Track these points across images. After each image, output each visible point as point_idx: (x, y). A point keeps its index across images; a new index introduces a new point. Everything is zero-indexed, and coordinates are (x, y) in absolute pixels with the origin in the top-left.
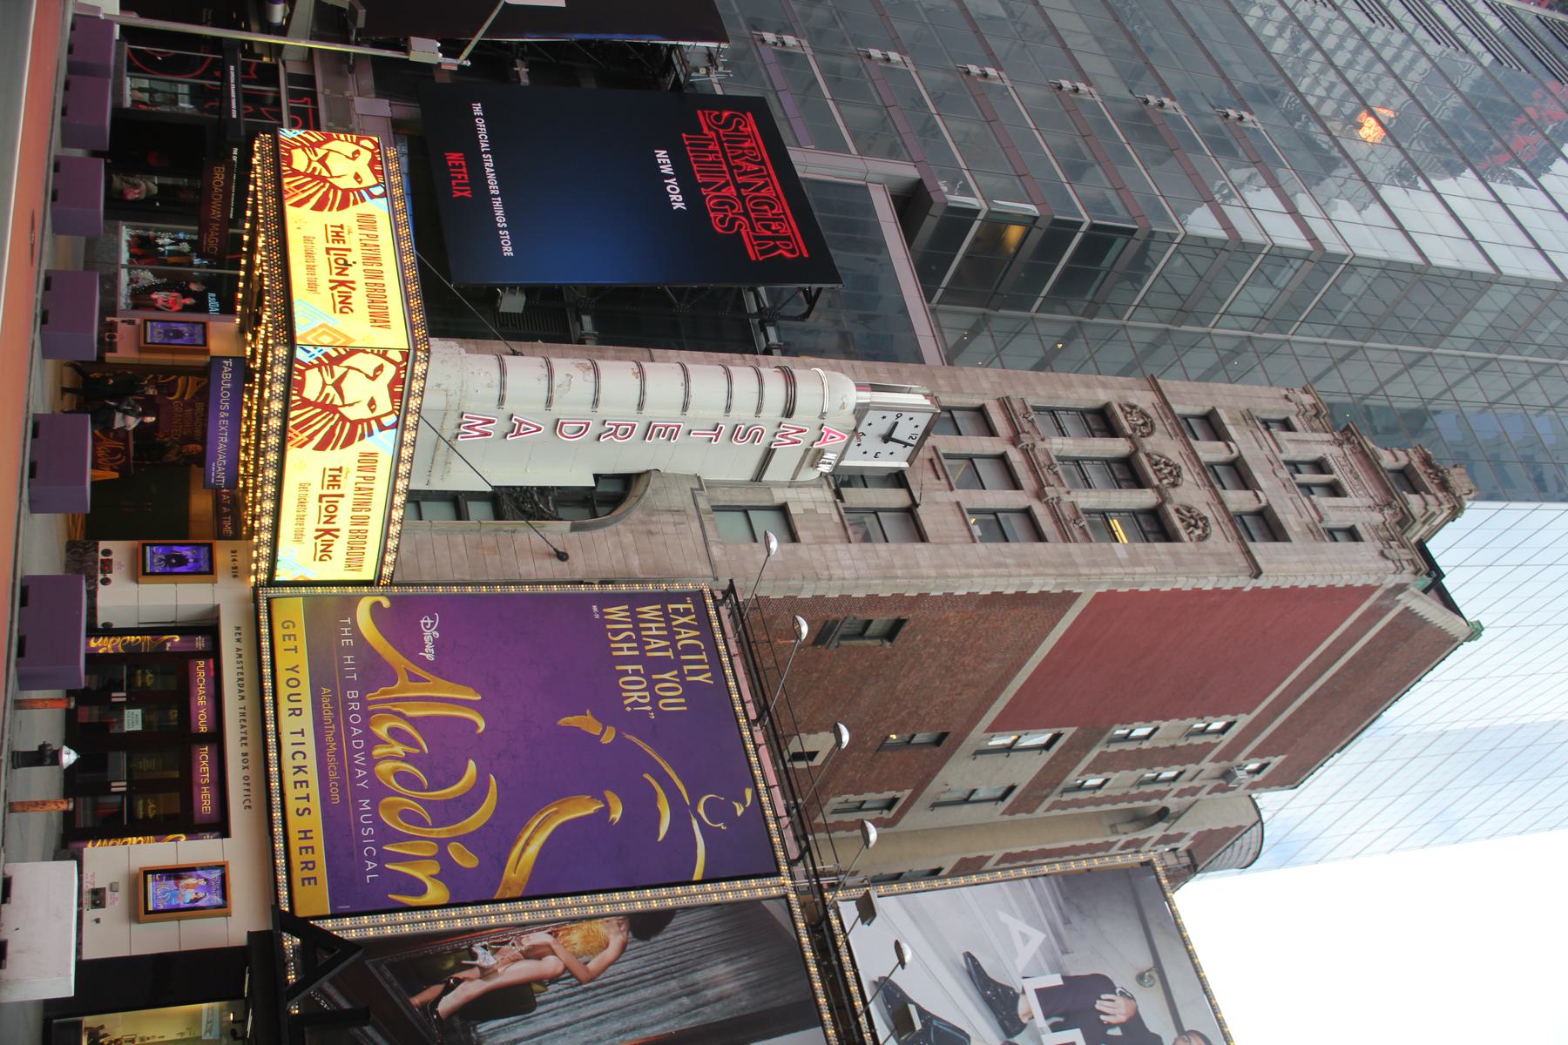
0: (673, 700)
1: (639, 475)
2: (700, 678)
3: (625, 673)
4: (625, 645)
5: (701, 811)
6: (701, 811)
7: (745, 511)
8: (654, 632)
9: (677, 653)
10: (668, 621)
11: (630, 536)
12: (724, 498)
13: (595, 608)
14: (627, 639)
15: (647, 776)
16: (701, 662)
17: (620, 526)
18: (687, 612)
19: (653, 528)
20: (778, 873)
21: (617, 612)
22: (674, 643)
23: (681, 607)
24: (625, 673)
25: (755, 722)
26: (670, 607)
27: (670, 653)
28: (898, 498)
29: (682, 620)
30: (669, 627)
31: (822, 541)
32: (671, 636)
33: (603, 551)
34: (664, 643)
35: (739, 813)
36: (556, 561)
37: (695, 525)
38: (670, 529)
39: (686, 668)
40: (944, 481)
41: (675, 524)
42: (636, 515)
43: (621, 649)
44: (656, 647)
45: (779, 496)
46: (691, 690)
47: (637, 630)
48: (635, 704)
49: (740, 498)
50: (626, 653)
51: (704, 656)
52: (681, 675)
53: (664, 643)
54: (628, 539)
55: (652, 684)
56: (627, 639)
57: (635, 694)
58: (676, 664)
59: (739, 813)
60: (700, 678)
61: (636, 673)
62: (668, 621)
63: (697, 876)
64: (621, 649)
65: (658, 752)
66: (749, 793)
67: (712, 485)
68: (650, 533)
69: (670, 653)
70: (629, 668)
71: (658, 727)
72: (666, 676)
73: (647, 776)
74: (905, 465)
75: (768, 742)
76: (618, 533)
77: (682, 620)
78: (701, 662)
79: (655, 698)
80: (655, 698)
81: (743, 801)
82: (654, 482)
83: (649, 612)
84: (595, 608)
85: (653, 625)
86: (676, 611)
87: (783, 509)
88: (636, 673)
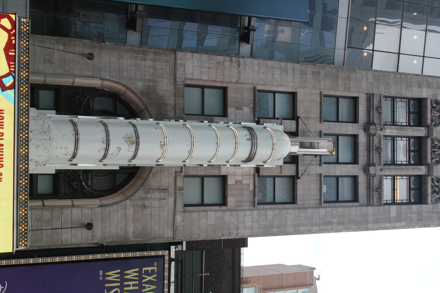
11: (132, 209)
13: (101, 273)
17: (128, 202)
19: (147, 203)
21: (113, 275)
23: (150, 269)
26: (144, 269)
29: (149, 278)
33: (114, 220)
36: (85, 231)
37: (171, 200)
38: (156, 203)
42: (140, 193)
54: (130, 211)
62: (140, 277)
68: (144, 207)
76: (125, 208)
77: (149, 278)
83: (132, 273)
84: (101, 273)
85: (131, 283)
86: (147, 273)
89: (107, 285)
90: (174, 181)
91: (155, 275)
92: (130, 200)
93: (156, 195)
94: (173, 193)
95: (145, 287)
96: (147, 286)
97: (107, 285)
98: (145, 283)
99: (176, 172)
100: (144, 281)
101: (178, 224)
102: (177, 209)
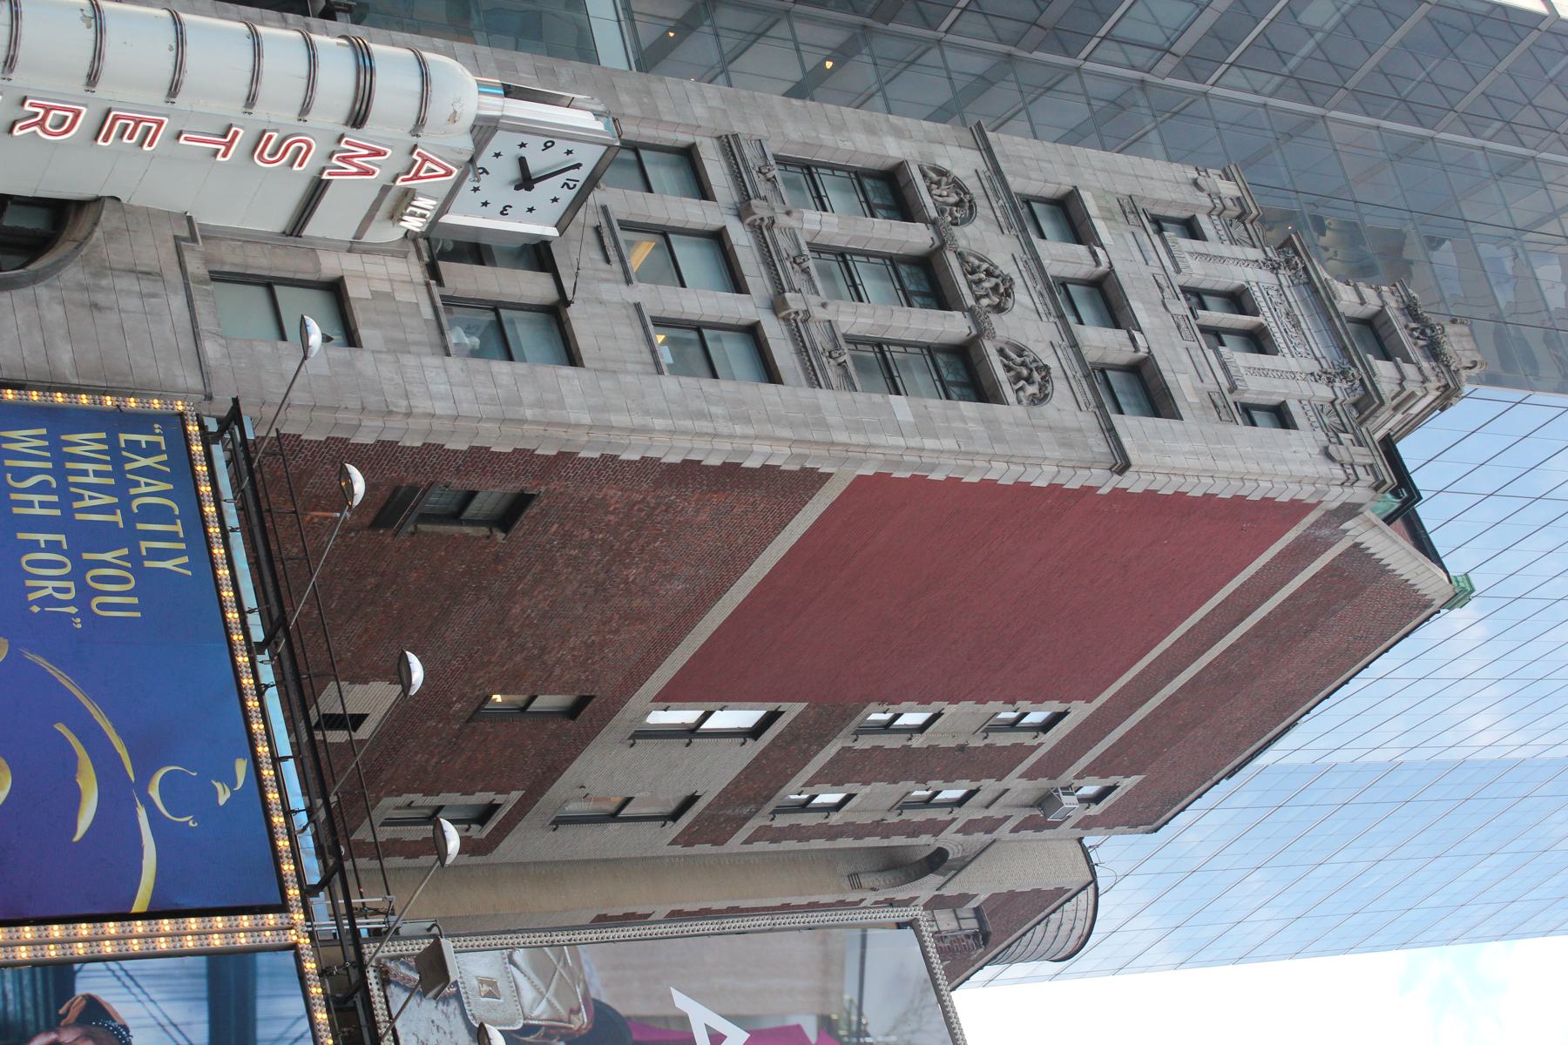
0: (117, 598)
1: (80, 205)
2: (168, 565)
3: (34, 546)
4: (36, 498)
5: (154, 793)
6: (154, 793)
7: (269, 284)
8: (92, 479)
9: (130, 518)
10: (118, 461)
11: (59, 310)
12: (232, 260)
14: (41, 488)
15: (60, 727)
16: (172, 537)
17: (41, 291)
18: (153, 449)
19: (101, 298)
20: (282, 907)
21: (26, 439)
22: (125, 501)
23: (143, 439)
24: (34, 546)
25: (261, 647)
26: (123, 437)
27: (118, 518)
28: (534, 287)
29: (143, 462)
30: (118, 473)
31: (399, 347)
32: (122, 488)
34: (107, 500)
35: (222, 801)
37: (178, 302)
38: (132, 303)
39: (144, 545)
40: (616, 266)
41: (142, 295)
42: (73, 274)
43: (30, 504)
44: (93, 505)
45: (330, 265)
46: (150, 584)
47: (60, 472)
48: (49, 601)
49: (262, 262)
50: (37, 511)
51: (178, 528)
52: (135, 558)
53: (107, 500)
54: (54, 314)
55: (81, 568)
56: (41, 488)
57: (48, 583)
58: (126, 537)
59: (223, 797)
60: (168, 565)
61: (53, 547)
62: (118, 461)
63: (140, 905)
64: (30, 504)
65: (83, 687)
66: (241, 768)
67: (213, 235)
68: (95, 306)
69: (118, 518)
70: (42, 538)
71: (84, 641)
72: (108, 557)
73: (60, 727)
74: (552, 232)
75: (280, 683)
77: (143, 462)
78: (172, 537)
79: (85, 593)
80: (85, 593)
81: (232, 782)
82: (109, 220)
83: (85, 443)
85: (90, 467)
86: (133, 446)
87: (335, 290)
88: (53, 547)
89: (8, 463)
90: (175, 257)
91: (164, 457)
92: (47, 286)
93: (127, 283)
94: (181, 286)
95: (137, 484)
96: (143, 480)
97: (8, 463)
98: (132, 472)
99: (176, 238)
100: (128, 466)
101: (212, 363)
102: (202, 326)
